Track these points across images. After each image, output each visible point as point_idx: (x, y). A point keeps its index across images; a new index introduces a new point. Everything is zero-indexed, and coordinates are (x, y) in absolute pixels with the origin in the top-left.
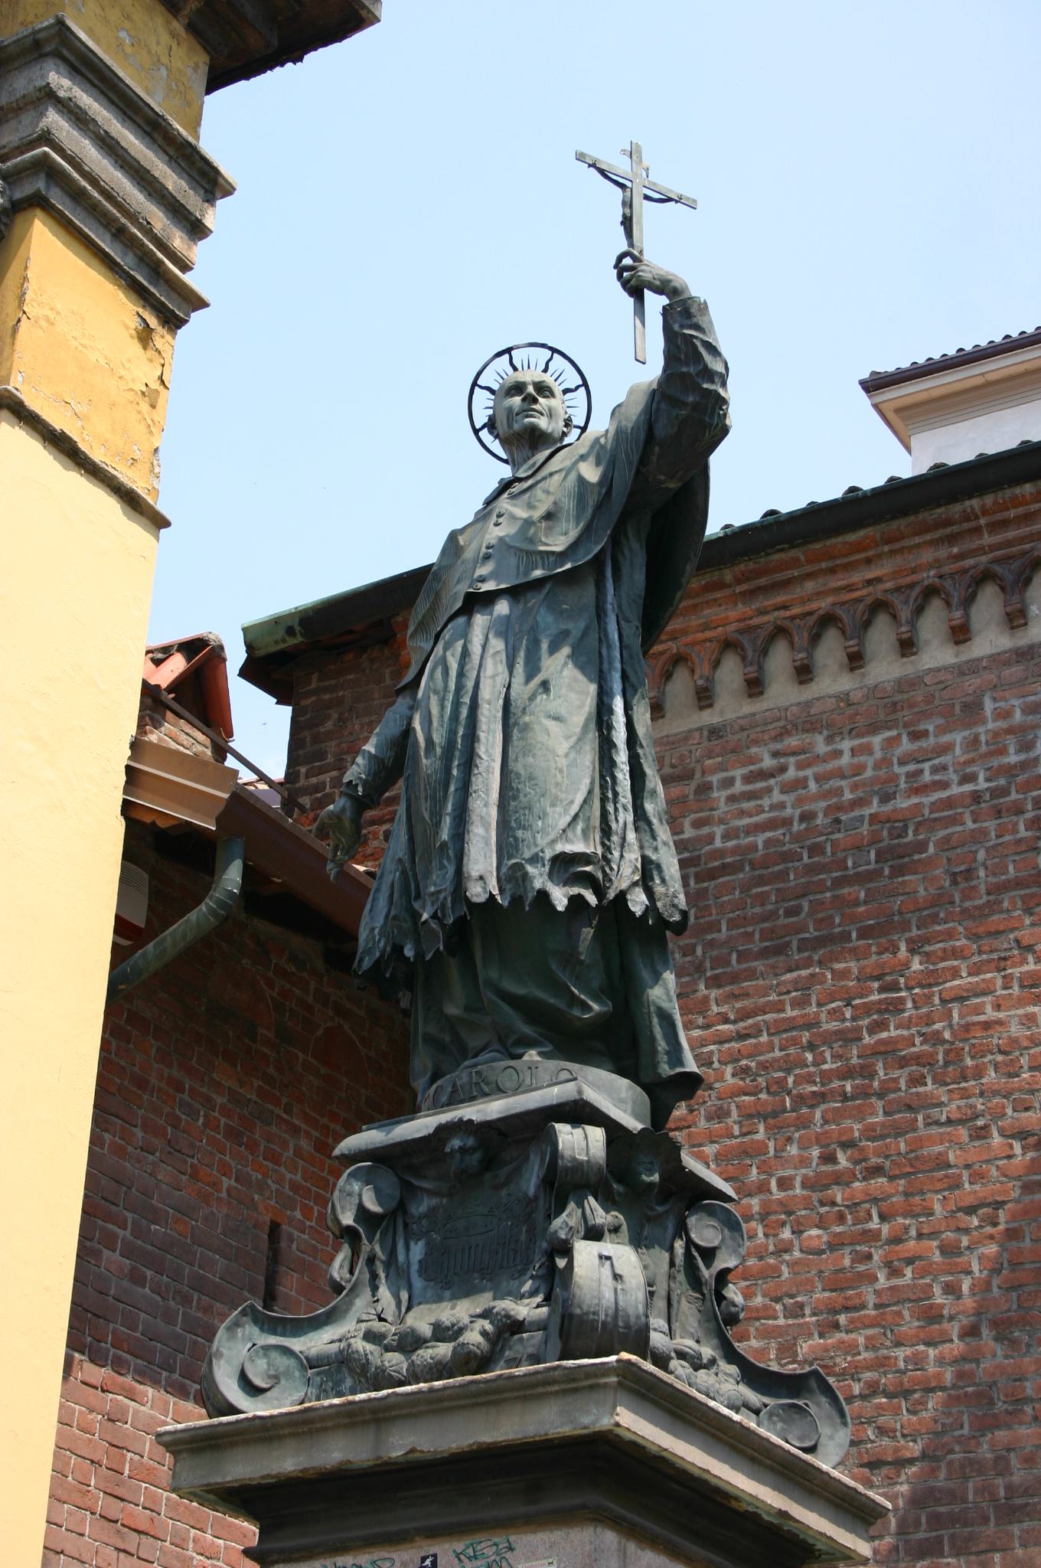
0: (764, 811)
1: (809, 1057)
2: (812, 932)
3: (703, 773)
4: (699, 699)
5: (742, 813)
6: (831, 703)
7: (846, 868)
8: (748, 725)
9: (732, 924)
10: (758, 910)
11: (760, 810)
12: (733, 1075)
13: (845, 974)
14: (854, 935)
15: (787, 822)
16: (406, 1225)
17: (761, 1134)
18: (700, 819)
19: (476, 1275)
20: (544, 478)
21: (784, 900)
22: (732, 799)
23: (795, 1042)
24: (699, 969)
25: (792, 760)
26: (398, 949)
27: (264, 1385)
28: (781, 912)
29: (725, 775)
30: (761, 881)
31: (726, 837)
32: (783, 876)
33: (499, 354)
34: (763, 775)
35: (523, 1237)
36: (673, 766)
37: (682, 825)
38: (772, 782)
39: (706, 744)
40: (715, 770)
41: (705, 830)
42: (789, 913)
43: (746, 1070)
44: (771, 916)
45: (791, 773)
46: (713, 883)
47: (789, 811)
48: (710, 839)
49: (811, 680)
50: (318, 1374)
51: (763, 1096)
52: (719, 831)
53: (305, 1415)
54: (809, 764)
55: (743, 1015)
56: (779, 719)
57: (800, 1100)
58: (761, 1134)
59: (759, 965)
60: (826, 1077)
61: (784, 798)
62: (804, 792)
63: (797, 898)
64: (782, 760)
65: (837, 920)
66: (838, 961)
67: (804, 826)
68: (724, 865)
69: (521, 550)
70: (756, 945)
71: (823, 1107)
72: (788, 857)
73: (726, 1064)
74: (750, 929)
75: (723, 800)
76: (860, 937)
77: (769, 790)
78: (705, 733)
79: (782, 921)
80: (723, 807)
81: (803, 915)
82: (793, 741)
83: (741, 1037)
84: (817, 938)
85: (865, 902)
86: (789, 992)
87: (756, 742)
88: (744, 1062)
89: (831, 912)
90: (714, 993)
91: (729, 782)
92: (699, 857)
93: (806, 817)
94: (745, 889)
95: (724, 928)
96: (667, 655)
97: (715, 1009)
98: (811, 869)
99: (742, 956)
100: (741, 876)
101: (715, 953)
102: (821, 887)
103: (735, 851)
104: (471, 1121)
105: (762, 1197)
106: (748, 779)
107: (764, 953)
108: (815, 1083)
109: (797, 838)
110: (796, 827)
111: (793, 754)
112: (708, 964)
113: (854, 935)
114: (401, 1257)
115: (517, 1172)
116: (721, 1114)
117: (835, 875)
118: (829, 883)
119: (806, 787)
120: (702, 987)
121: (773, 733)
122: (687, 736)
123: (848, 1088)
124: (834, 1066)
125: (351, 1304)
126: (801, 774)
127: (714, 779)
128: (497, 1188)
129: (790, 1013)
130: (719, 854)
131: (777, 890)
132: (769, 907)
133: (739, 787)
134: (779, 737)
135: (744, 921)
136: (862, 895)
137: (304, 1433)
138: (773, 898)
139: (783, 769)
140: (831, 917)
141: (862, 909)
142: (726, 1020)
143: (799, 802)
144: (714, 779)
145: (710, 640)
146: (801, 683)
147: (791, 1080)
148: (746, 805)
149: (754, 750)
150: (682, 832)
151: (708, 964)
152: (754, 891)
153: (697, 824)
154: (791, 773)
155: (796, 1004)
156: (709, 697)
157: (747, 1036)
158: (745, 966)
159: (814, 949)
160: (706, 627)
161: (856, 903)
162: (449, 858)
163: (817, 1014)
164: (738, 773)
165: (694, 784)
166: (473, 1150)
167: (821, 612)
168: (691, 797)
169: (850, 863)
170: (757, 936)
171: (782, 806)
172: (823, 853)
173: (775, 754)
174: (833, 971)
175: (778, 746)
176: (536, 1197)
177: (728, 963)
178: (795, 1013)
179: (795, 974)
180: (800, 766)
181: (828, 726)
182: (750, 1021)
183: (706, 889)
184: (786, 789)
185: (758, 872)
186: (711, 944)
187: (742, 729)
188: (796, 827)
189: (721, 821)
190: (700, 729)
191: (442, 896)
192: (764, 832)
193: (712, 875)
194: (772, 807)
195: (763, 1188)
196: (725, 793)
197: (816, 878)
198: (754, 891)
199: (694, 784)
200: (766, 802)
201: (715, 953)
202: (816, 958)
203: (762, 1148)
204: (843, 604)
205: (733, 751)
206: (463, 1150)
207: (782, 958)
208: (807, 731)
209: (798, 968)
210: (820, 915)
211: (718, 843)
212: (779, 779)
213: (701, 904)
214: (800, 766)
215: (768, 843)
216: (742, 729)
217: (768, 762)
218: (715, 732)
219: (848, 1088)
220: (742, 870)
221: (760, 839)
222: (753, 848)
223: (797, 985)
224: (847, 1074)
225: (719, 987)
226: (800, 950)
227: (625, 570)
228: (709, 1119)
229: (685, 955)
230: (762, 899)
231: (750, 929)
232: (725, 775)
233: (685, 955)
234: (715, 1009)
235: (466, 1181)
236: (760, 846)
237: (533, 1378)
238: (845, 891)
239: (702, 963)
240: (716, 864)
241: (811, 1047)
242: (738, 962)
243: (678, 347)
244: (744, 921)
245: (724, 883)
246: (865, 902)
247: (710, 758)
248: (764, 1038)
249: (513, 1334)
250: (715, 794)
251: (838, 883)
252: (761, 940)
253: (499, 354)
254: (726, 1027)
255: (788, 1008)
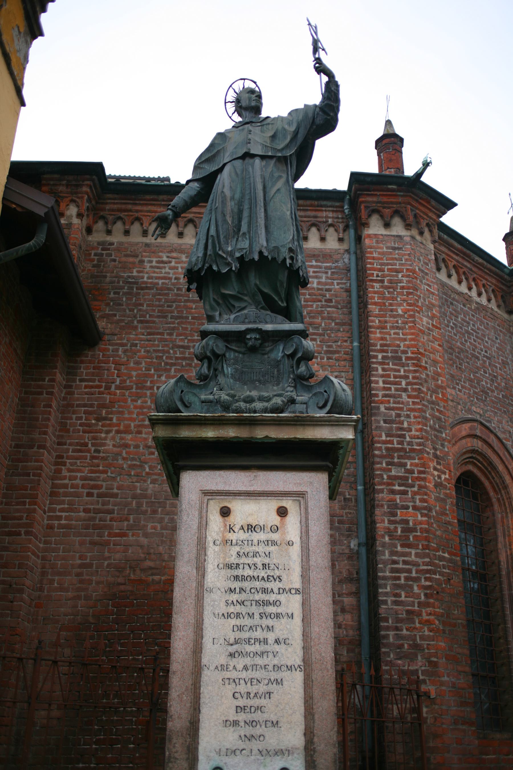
0: (162, 273)
1: (171, 352)
2: (176, 314)
3: (142, 257)
4: (143, 233)
5: (154, 272)
6: (188, 246)
7: (189, 297)
8: (160, 246)
9: (148, 305)
10: (157, 303)
11: (161, 273)
12: (144, 352)
13: (186, 329)
14: (190, 318)
15: (170, 279)
16: (226, 361)
17: (152, 371)
18: (140, 270)
19: (257, 382)
20: (266, 124)
21: (167, 302)
22: (151, 267)
23: (167, 345)
24: (135, 317)
25: (174, 260)
26: (211, 267)
27: (189, 406)
28: (166, 305)
29: (149, 259)
30: (160, 294)
31: (148, 278)
32: (167, 295)
33: (241, 79)
34: (163, 262)
35: (276, 373)
36: (131, 252)
37: (133, 271)
38: (166, 265)
39: (143, 248)
40: (146, 257)
41: (141, 274)
42: (168, 306)
43: (148, 352)
44: (162, 306)
45: (173, 264)
46: (142, 291)
47: (171, 275)
48: (143, 277)
49: (182, 238)
50: (205, 405)
51: (154, 360)
52: (146, 276)
53: (221, 418)
54: (179, 263)
55: (149, 334)
56: (170, 247)
57: (166, 364)
58: (152, 371)
59: (156, 320)
60: (177, 358)
61: (170, 271)
62: (177, 271)
63: (171, 302)
64: (170, 259)
65: (185, 312)
66: (183, 324)
67: (176, 281)
68: (147, 287)
69: (263, 145)
70: (156, 314)
71: (175, 367)
72: (169, 289)
73: (142, 348)
74: (154, 308)
75: (148, 266)
76: (192, 319)
77: (165, 267)
78: (144, 245)
79: (166, 308)
80: (148, 269)
81: (173, 308)
82: (174, 255)
83: (148, 340)
84: (177, 316)
85: (195, 309)
86: (166, 330)
87: (162, 252)
88: (148, 349)
89: (183, 309)
90: (140, 325)
91: (151, 262)
92: (138, 282)
93: (176, 278)
94: (154, 295)
95: (145, 306)
96: (134, 217)
97: (139, 330)
98: (177, 295)
99: (150, 316)
100: (153, 291)
101: (141, 313)
102: (180, 301)
103: (151, 283)
104: (261, 329)
105: (151, 391)
106: (158, 262)
107: (158, 317)
108: (172, 360)
109: (173, 284)
110: (173, 281)
111: (174, 258)
112: (138, 316)
113: (190, 318)
114: (226, 371)
115: (272, 350)
116: (137, 363)
117: (185, 298)
118: (183, 300)
119: (178, 269)
120: (135, 322)
121: (168, 250)
122: (137, 244)
123: (184, 363)
124: (180, 356)
125: (209, 383)
126: (177, 265)
127: (146, 259)
128: (264, 354)
129: (166, 336)
130: (146, 283)
131: (165, 299)
132: (161, 303)
133: (154, 264)
134: (171, 251)
135: (153, 306)
136: (194, 306)
137: (217, 424)
138: (163, 301)
139: (170, 262)
140: (183, 311)
141: (193, 311)
142: (143, 335)
143: (175, 273)
144: (146, 259)
145: (149, 216)
146: (179, 238)
147: (164, 358)
148: (156, 270)
149: (160, 254)
150: (133, 273)
151: (138, 316)
152: (157, 297)
153: (138, 272)
154: (173, 264)
155: (168, 334)
156: (147, 234)
157: (150, 341)
158: (151, 319)
159: (176, 319)
160: (149, 211)
161: (192, 308)
162: (246, 239)
163: (176, 339)
164: (155, 260)
165: (138, 259)
166: (259, 339)
167: (189, 218)
168: (137, 263)
169: (191, 296)
170: (156, 311)
171: (169, 273)
172: (182, 291)
173: (168, 257)
174: (182, 327)
175: (169, 255)
176: (280, 360)
177: (145, 317)
178: (168, 337)
179: (169, 325)
180: (176, 263)
181: (187, 253)
182: (152, 336)
183: (140, 293)
184: (171, 268)
185: (158, 291)
186: (140, 310)
187: (157, 246)
188: (173, 281)
189: (147, 273)
190: (142, 243)
191: (245, 251)
192: (162, 279)
193: (142, 289)
194: (165, 273)
195: (151, 388)
196: (149, 265)
197: (179, 298)
198: (157, 297)
199: (138, 259)
200: (163, 271)
201: (141, 313)
202: (176, 322)
203: (152, 376)
204: (197, 217)
205: (153, 252)
206: (256, 339)
207: (165, 319)
208: (179, 253)
209: (170, 324)
210: (179, 309)
211: (145, 279)
212: (168, 265)
213: (138, 297)
214: (176, 263)
215: (163, 283)
216: (157, 246)
217: (165, 259)
218: (147, 245)
219: (184, 363)
220: (153, 289)
221: (160, 282)
222: (157, 284)
223: (169, 329)
224: (184, 358)
225: (142, 323)
226: (171, 318)
227: (293, 162)
228: (134, 364)
229: (130, 311)
230: (159, 300)
231: (154, 308)
232: (149, 259)
233: (130, 311)
234: (139, 330)
235: (253, 350)
236: (160, 283)
237: (322, 419)
238: (188, 304)
239: (136, 315)
240: (144, 285)
241: (172, 348)
242: (149, 317)
243: (332, 96)
244: (153, 306)
245: (146, 292)
246: (195, 309)
247: (145, 252)
248: (156, 343)
249: (292, 403)
250: (146, 264)
251: (186, 301)
252: (158, 312)
253: (241, 79)
254: (143, 336)
255: (165, 335)
